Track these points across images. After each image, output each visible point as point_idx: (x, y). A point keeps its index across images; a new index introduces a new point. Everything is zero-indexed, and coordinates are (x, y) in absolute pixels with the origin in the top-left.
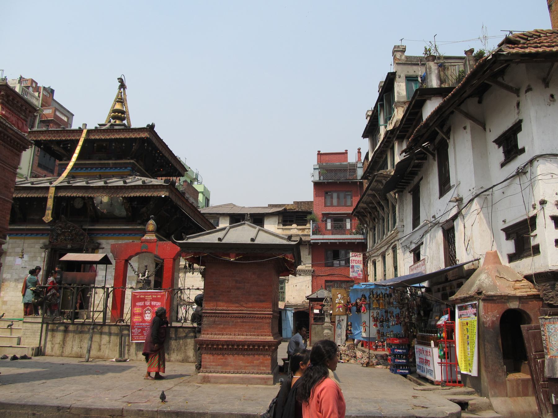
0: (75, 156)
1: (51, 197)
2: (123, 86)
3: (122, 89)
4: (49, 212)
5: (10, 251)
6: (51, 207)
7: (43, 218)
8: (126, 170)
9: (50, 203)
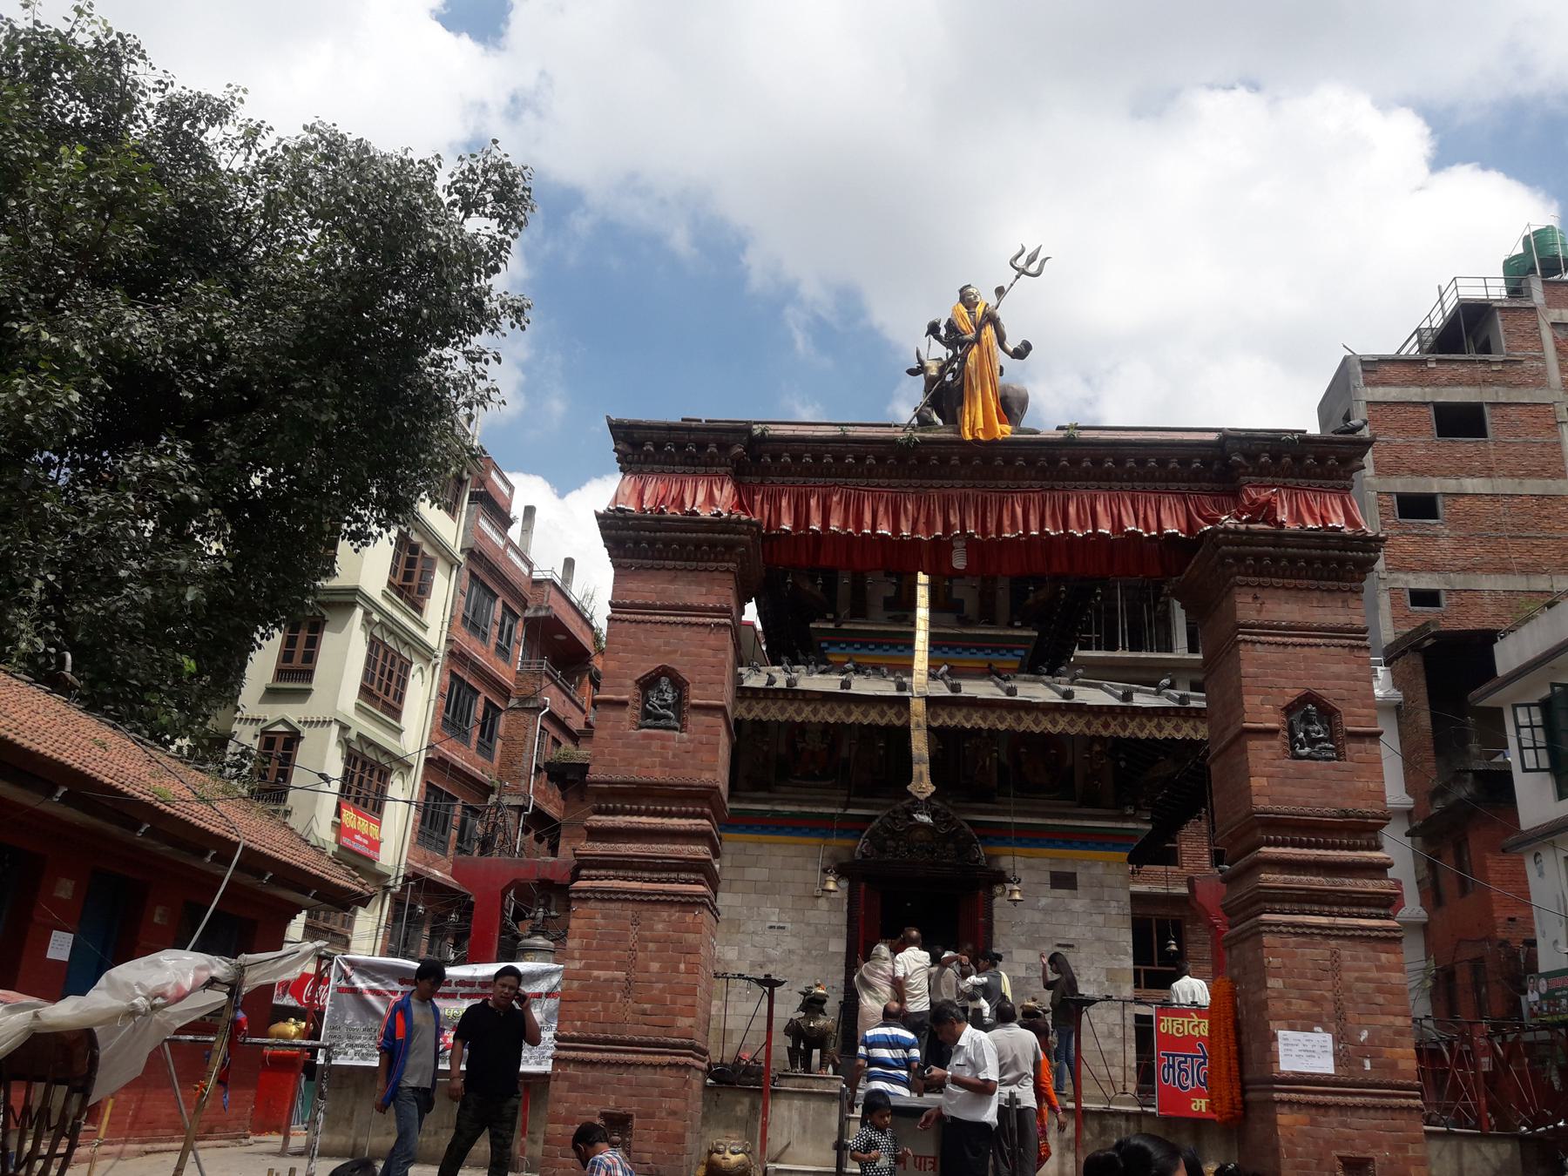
0: (922, 612)
1: (918, 725)
4: (921, 769)
5: (725, 876)
6: (926, 754)
7: (909, 788)
8: (1009, 656)
9: (920, 745)
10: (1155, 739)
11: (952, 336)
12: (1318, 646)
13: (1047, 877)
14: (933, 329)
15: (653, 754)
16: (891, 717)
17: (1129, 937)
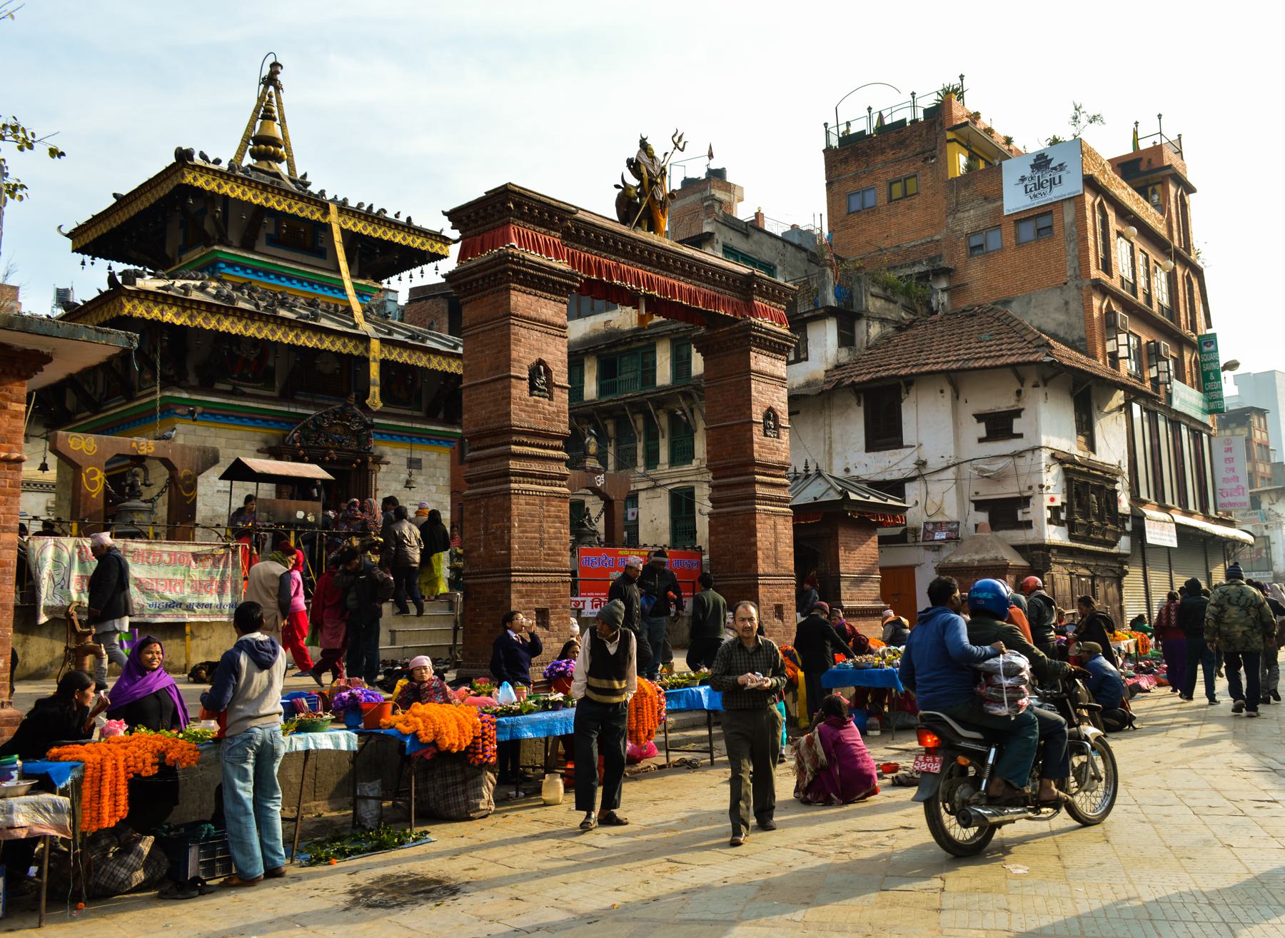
2: (271, 80)
3: (271, 89)
4: (375, 390)
11: (634, 166)
13: (405, 461)
16: (350, 348)
17: (449, 500)
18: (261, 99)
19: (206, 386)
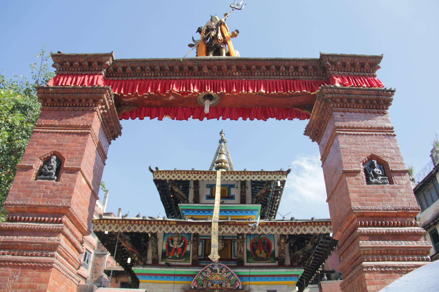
7: (209, 257)
10: (303, 234)
12: (372, 135)
14: (199, 31)
15: (40, 192)
18: (219, 148)
19: (155, 263)
